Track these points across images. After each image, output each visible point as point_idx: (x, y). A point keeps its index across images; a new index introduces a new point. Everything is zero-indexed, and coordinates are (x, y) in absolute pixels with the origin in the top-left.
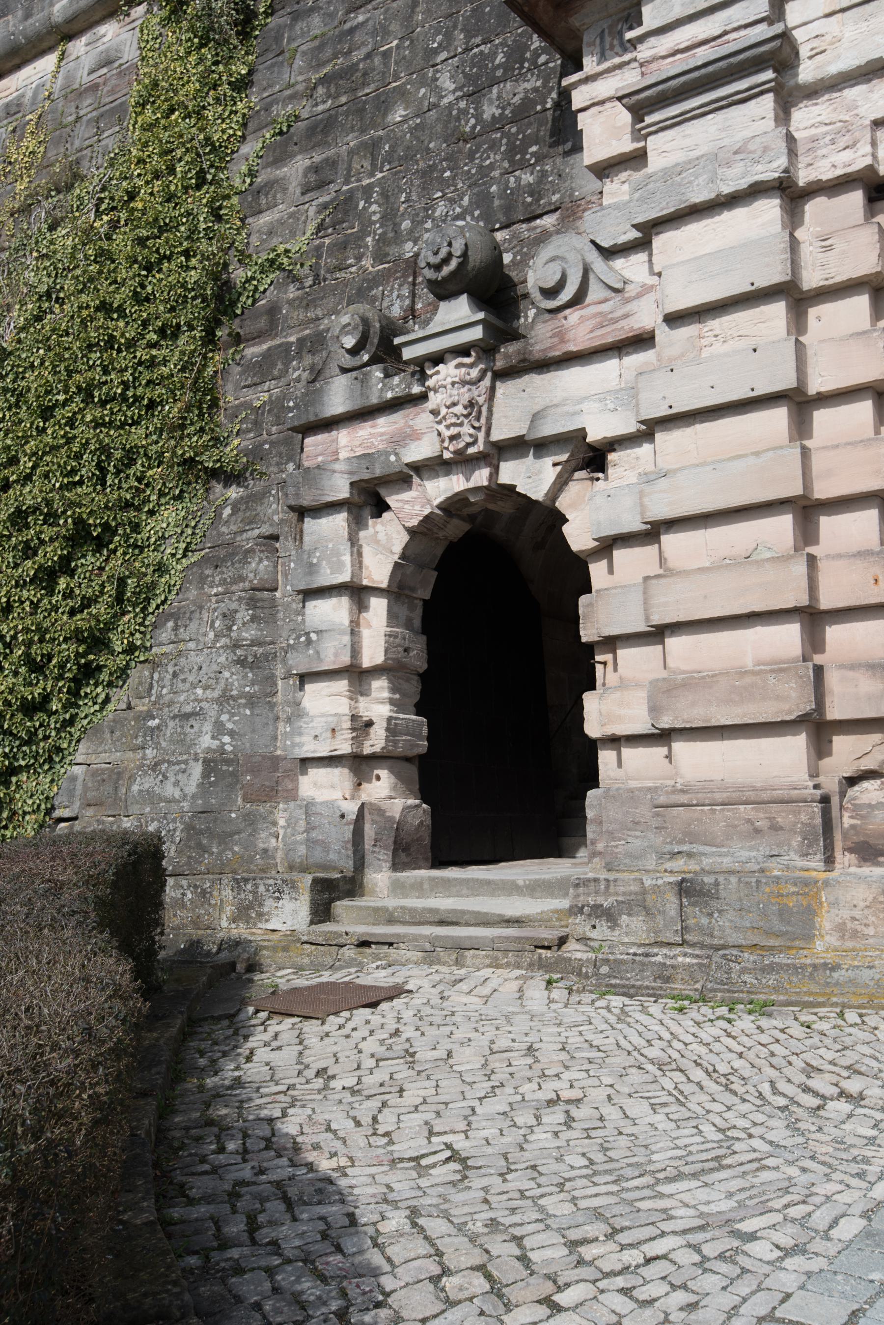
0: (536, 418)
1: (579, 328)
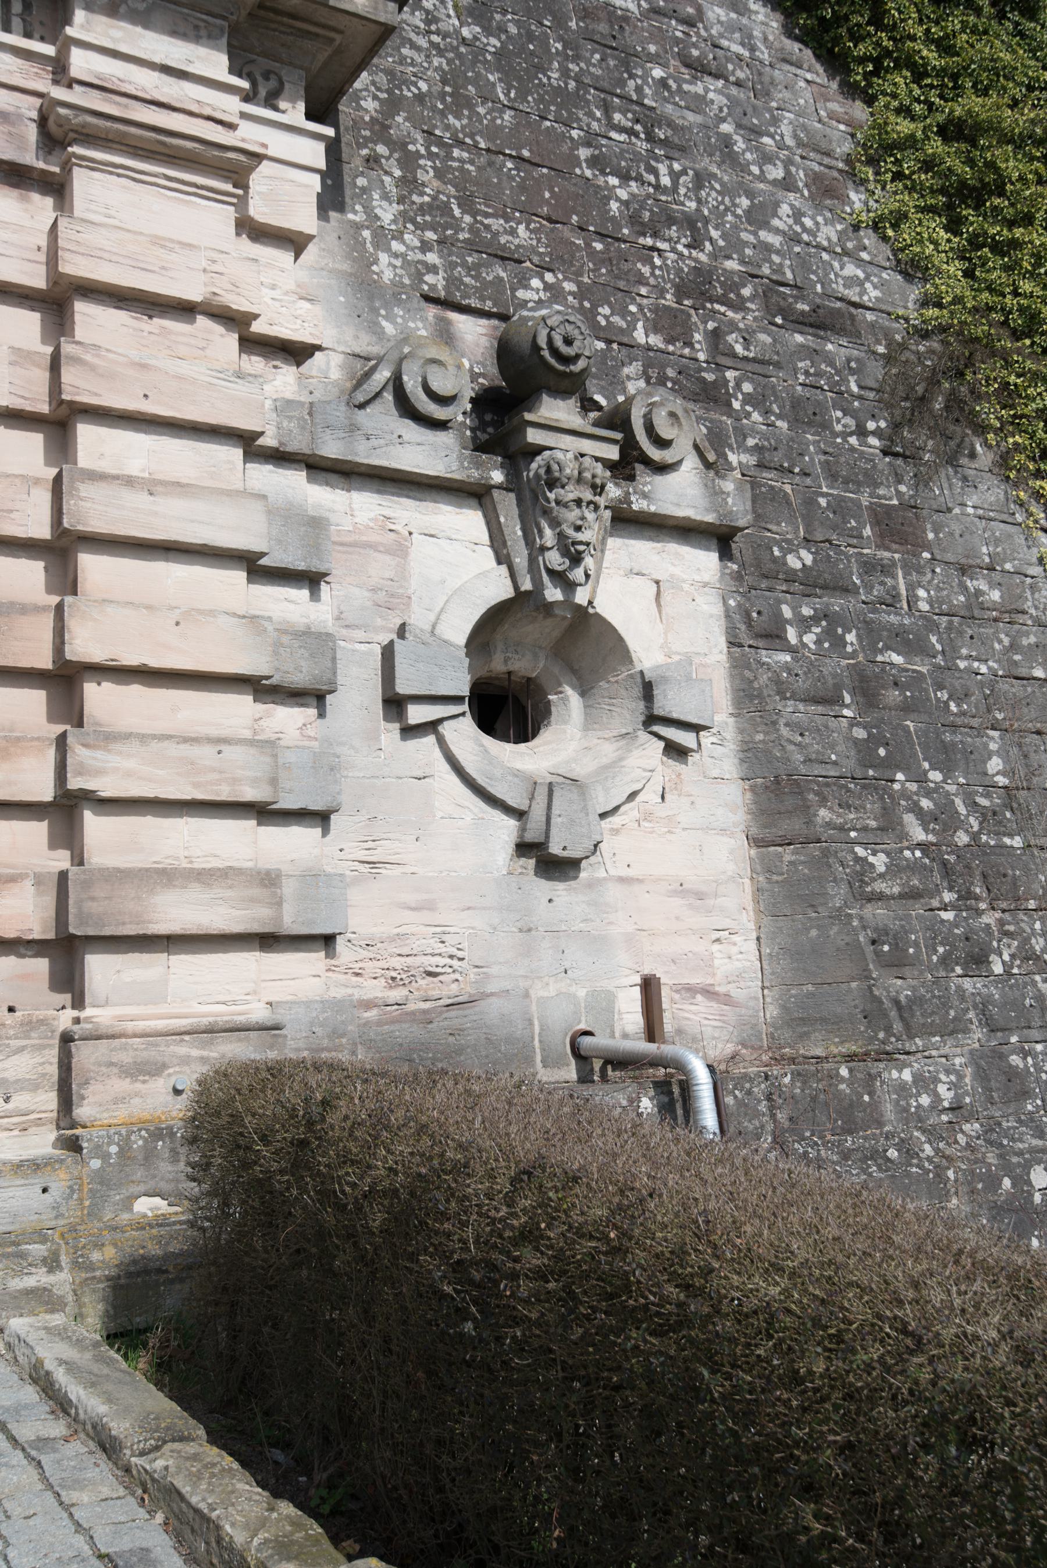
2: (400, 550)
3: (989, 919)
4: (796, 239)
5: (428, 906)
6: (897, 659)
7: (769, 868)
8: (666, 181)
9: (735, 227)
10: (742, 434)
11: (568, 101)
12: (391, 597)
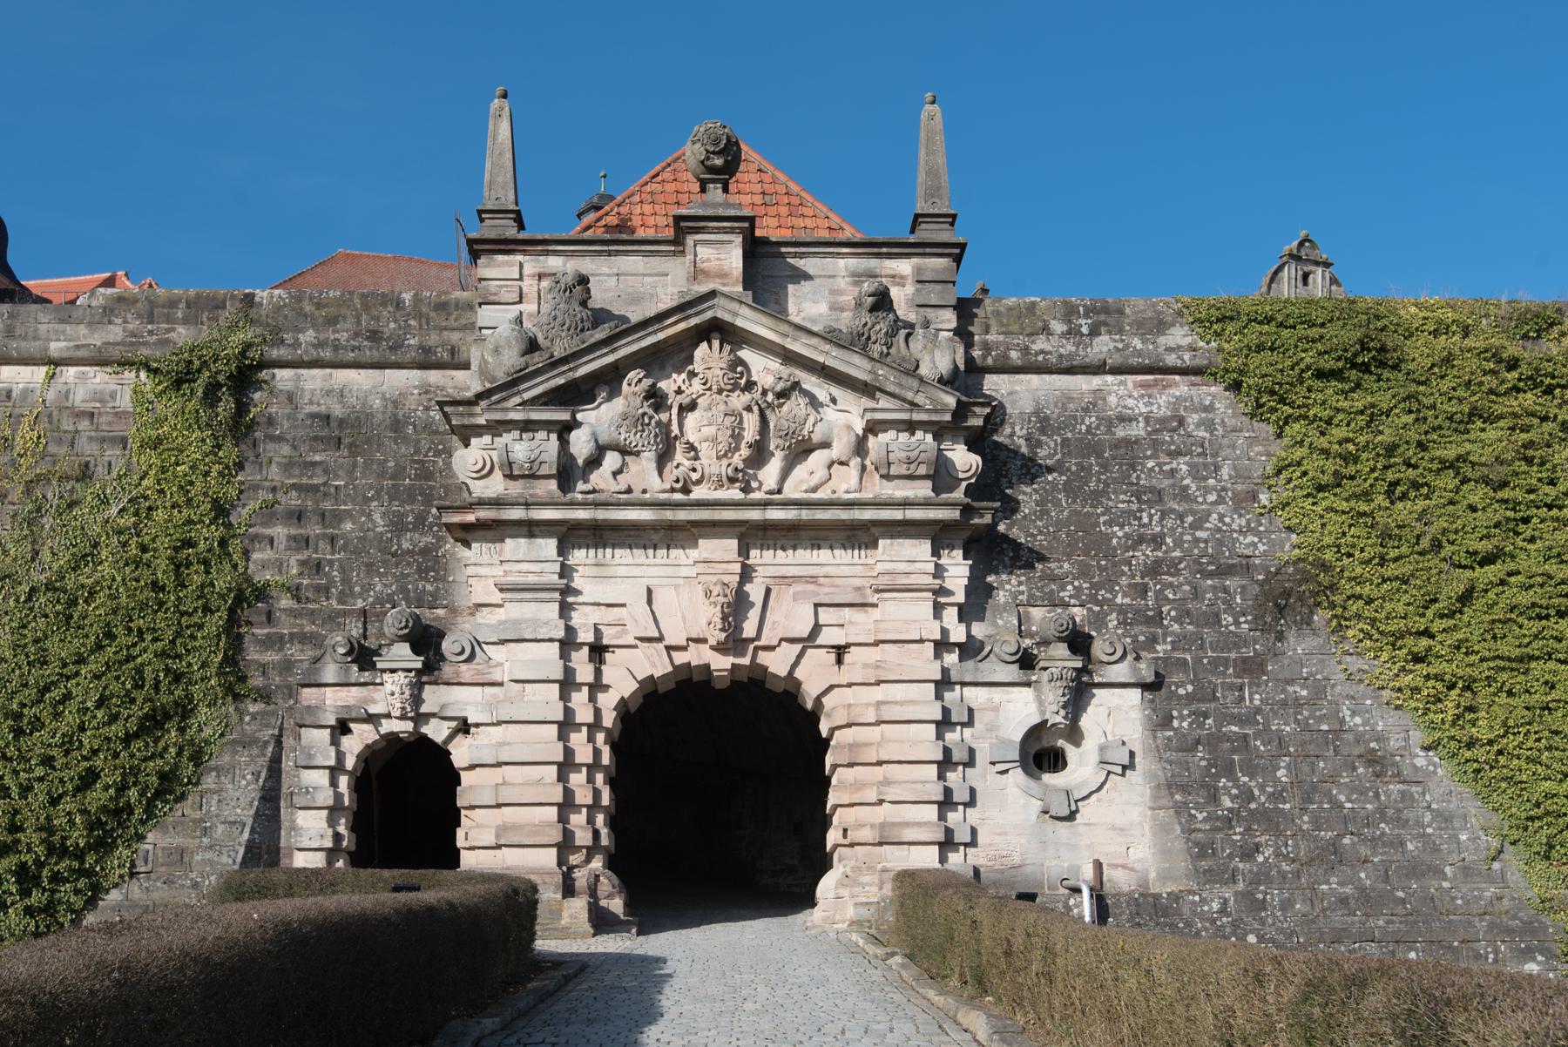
0: (443, 707)
1: (467, 672)
2: (996, 709)
3: (1263, 839)
4: (1219, 530)
5: (1004, 834)
6: (1234, 728)
7: (1154, 818)
8: (1146, 520)
9: (1182, 534)
10: (1165, 635)
11: (1097, 496)
12: (992, 728)
